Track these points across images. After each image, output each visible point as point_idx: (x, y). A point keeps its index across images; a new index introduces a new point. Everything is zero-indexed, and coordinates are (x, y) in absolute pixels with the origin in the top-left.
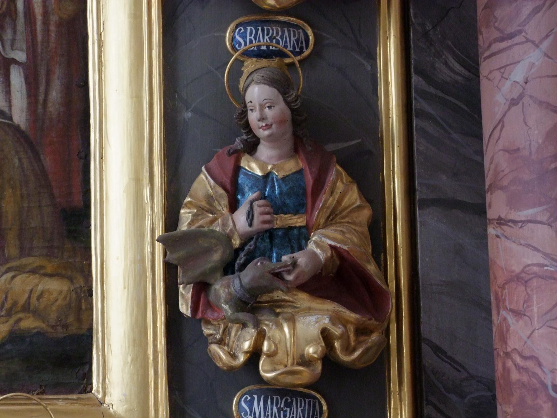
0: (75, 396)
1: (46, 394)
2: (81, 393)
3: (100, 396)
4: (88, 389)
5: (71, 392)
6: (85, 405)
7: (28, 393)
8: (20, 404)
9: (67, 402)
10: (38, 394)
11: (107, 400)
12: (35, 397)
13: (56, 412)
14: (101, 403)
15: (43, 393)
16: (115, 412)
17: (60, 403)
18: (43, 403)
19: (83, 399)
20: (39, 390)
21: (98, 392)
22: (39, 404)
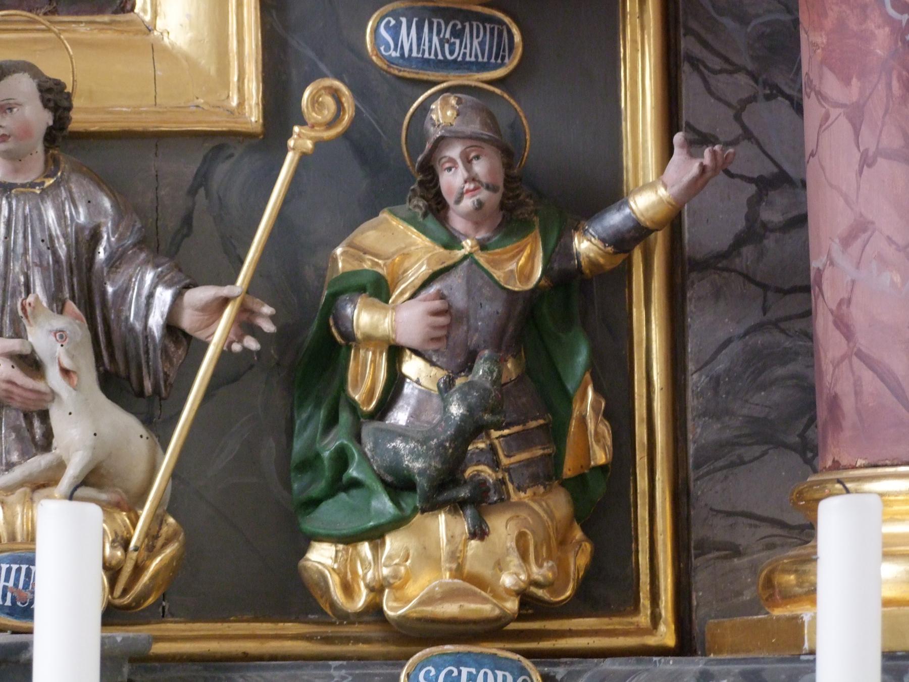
0: (106, 18)
1: (59, 14)
2: (116, 12)
3: (147, 18)
4: (129, 7)
5: (101, 11)
6: (122, 32)
7: (30, 11)
8: (16, 30)
9: (93, 27)
10: (45, 14)
11: (160, 24)
12: (40, 18)
13: (75, 43)
14: (149, 29)
15: (54, 12)
16: (173, 45)
17: (82, 28)
18: (56, 28)
19: (119, 22)
20: (47, 8)
21: (144, 11)
22: (49, 30)
